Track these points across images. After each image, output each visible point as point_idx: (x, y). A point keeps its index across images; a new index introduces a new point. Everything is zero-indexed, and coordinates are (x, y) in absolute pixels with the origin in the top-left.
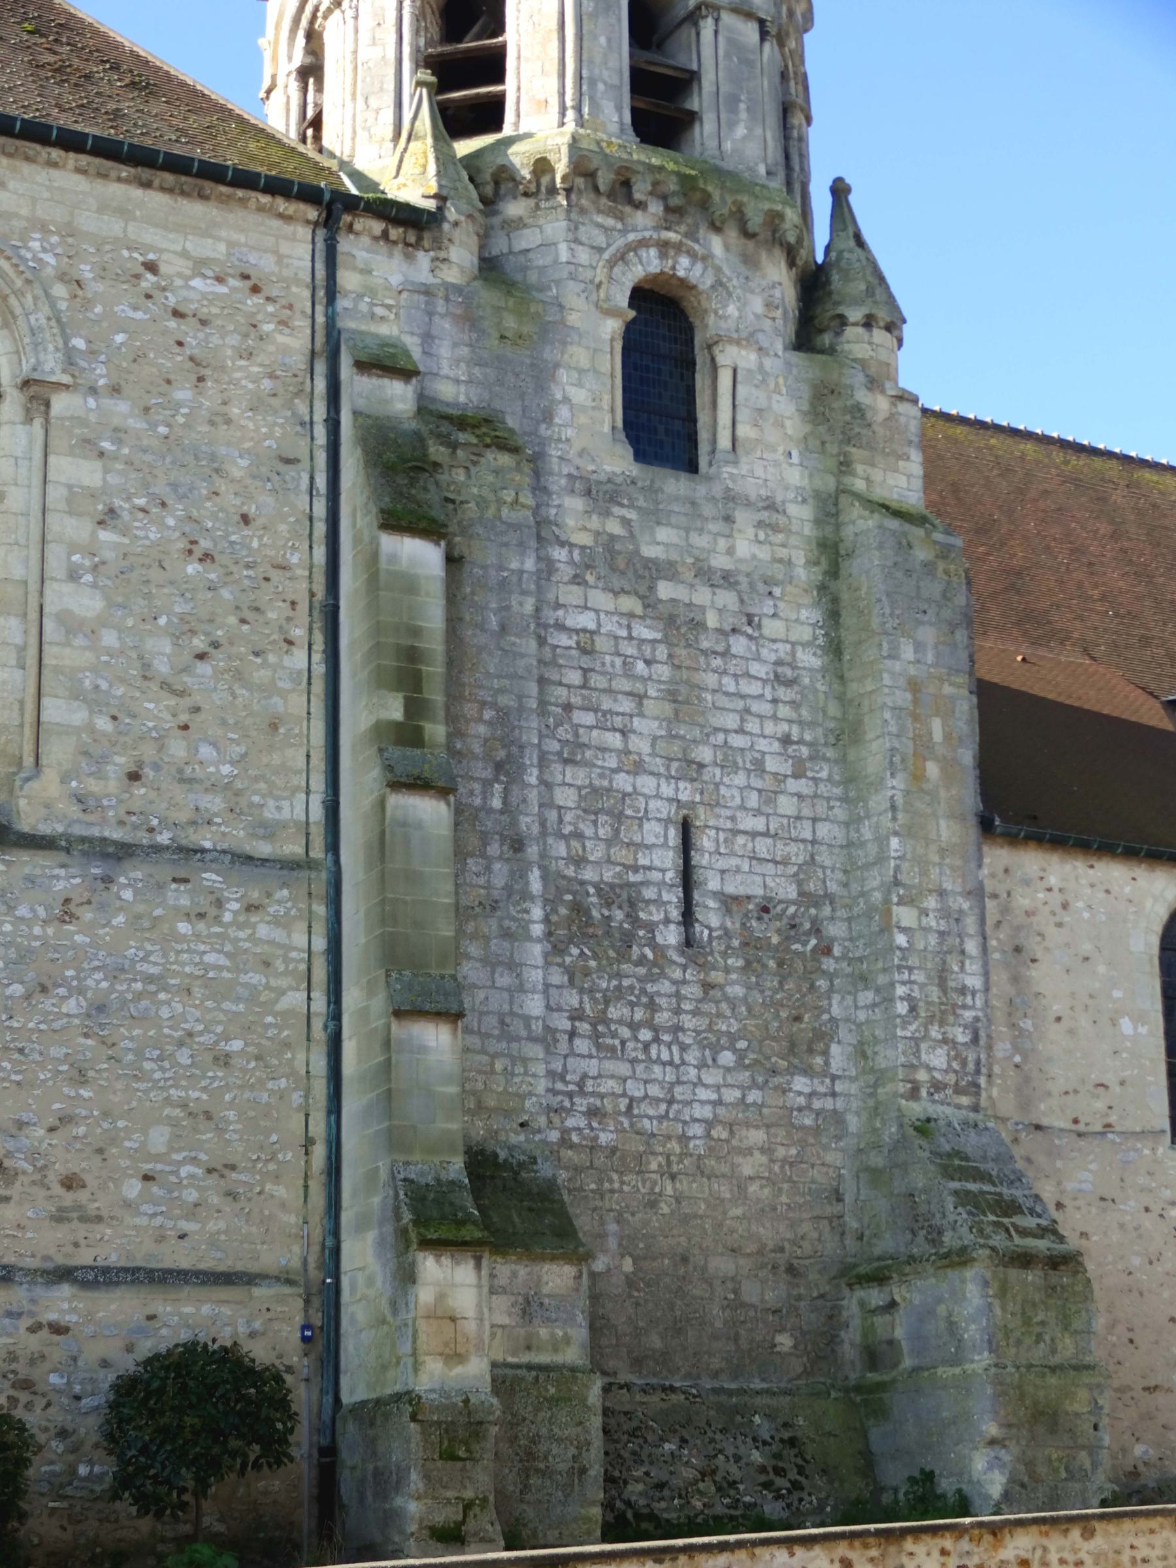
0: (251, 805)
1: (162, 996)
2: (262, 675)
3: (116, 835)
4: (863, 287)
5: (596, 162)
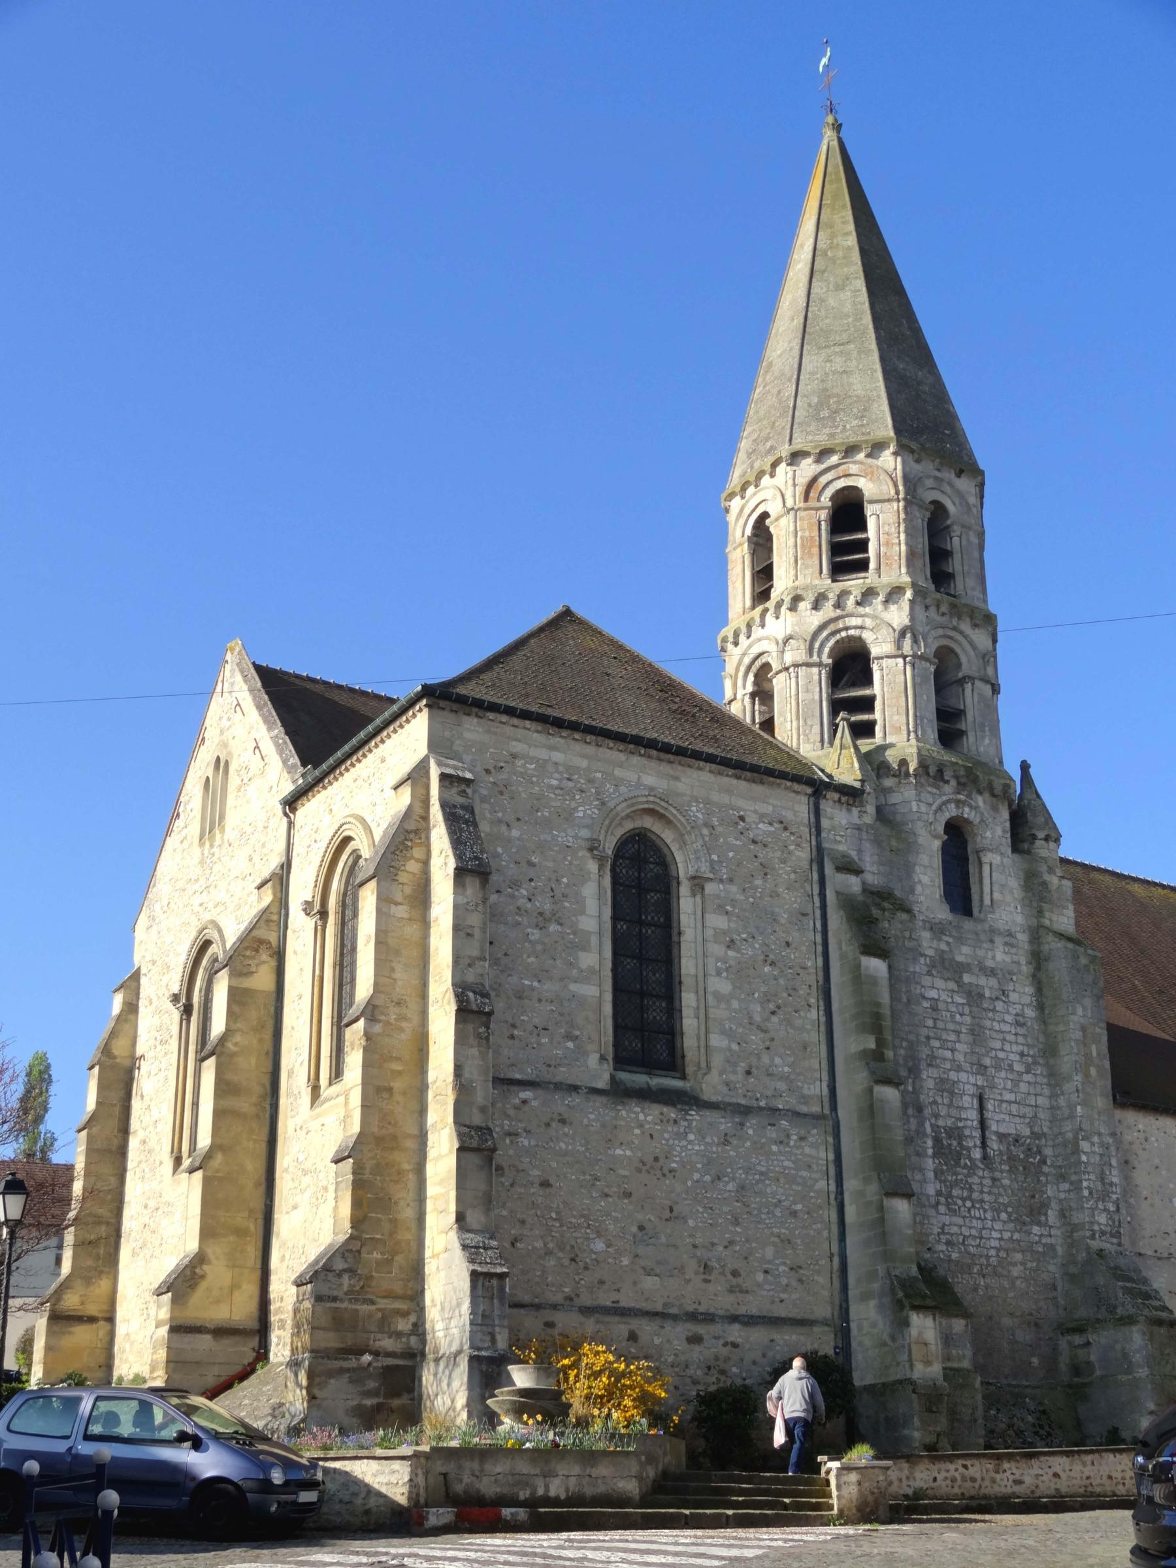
0: (798, 1087)
1: (767, 1182)
2: (798, 1022)
3: (743, 1102)
4: (1043, 820)
5: (929, 762)
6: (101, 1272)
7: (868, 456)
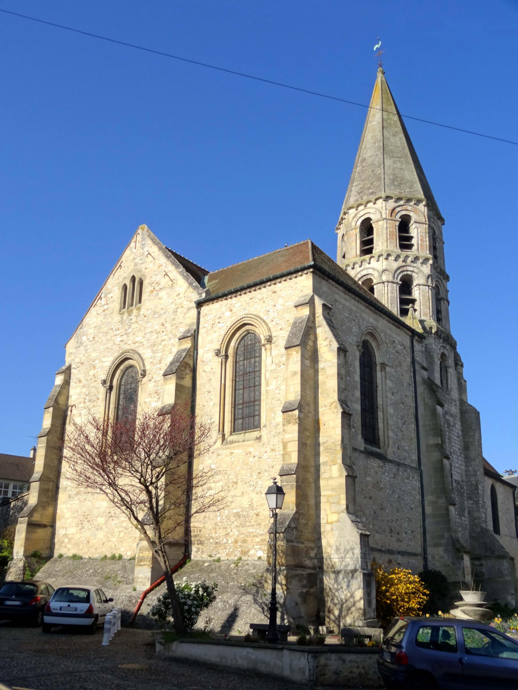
6: (49, 504)
7: (415, 204)
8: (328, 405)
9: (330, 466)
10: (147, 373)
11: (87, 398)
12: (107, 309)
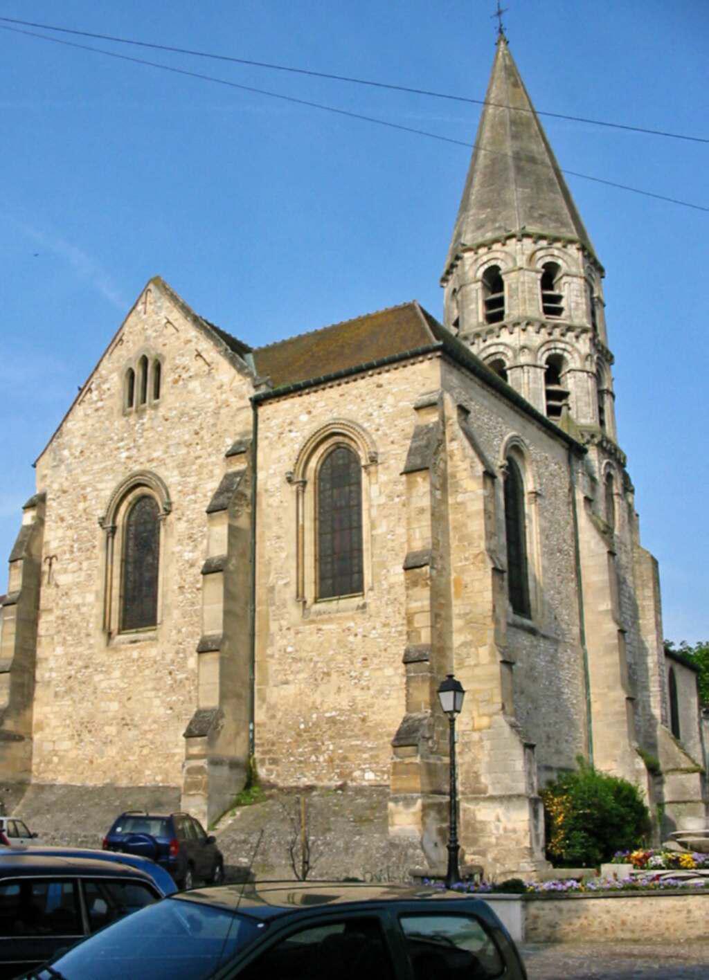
8: (471, 557)
9: (476, 648)
10: (174, 506)
11: (76, 546)
12: (102, 407)
